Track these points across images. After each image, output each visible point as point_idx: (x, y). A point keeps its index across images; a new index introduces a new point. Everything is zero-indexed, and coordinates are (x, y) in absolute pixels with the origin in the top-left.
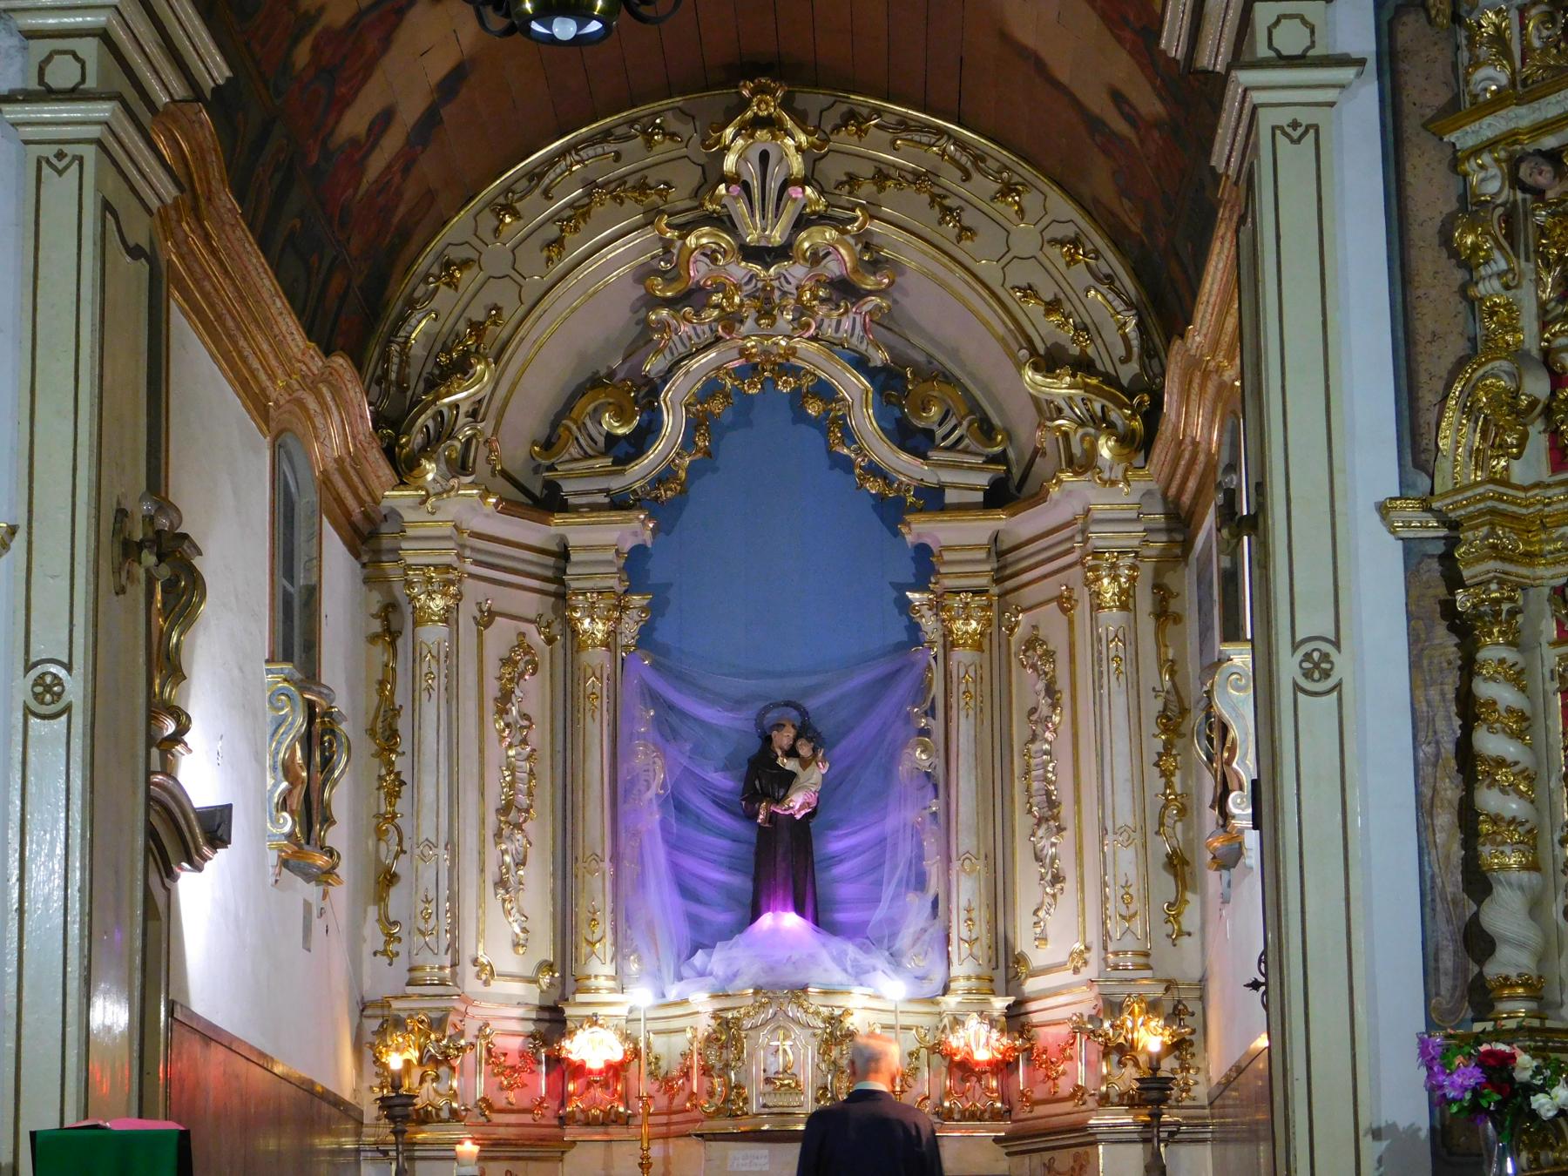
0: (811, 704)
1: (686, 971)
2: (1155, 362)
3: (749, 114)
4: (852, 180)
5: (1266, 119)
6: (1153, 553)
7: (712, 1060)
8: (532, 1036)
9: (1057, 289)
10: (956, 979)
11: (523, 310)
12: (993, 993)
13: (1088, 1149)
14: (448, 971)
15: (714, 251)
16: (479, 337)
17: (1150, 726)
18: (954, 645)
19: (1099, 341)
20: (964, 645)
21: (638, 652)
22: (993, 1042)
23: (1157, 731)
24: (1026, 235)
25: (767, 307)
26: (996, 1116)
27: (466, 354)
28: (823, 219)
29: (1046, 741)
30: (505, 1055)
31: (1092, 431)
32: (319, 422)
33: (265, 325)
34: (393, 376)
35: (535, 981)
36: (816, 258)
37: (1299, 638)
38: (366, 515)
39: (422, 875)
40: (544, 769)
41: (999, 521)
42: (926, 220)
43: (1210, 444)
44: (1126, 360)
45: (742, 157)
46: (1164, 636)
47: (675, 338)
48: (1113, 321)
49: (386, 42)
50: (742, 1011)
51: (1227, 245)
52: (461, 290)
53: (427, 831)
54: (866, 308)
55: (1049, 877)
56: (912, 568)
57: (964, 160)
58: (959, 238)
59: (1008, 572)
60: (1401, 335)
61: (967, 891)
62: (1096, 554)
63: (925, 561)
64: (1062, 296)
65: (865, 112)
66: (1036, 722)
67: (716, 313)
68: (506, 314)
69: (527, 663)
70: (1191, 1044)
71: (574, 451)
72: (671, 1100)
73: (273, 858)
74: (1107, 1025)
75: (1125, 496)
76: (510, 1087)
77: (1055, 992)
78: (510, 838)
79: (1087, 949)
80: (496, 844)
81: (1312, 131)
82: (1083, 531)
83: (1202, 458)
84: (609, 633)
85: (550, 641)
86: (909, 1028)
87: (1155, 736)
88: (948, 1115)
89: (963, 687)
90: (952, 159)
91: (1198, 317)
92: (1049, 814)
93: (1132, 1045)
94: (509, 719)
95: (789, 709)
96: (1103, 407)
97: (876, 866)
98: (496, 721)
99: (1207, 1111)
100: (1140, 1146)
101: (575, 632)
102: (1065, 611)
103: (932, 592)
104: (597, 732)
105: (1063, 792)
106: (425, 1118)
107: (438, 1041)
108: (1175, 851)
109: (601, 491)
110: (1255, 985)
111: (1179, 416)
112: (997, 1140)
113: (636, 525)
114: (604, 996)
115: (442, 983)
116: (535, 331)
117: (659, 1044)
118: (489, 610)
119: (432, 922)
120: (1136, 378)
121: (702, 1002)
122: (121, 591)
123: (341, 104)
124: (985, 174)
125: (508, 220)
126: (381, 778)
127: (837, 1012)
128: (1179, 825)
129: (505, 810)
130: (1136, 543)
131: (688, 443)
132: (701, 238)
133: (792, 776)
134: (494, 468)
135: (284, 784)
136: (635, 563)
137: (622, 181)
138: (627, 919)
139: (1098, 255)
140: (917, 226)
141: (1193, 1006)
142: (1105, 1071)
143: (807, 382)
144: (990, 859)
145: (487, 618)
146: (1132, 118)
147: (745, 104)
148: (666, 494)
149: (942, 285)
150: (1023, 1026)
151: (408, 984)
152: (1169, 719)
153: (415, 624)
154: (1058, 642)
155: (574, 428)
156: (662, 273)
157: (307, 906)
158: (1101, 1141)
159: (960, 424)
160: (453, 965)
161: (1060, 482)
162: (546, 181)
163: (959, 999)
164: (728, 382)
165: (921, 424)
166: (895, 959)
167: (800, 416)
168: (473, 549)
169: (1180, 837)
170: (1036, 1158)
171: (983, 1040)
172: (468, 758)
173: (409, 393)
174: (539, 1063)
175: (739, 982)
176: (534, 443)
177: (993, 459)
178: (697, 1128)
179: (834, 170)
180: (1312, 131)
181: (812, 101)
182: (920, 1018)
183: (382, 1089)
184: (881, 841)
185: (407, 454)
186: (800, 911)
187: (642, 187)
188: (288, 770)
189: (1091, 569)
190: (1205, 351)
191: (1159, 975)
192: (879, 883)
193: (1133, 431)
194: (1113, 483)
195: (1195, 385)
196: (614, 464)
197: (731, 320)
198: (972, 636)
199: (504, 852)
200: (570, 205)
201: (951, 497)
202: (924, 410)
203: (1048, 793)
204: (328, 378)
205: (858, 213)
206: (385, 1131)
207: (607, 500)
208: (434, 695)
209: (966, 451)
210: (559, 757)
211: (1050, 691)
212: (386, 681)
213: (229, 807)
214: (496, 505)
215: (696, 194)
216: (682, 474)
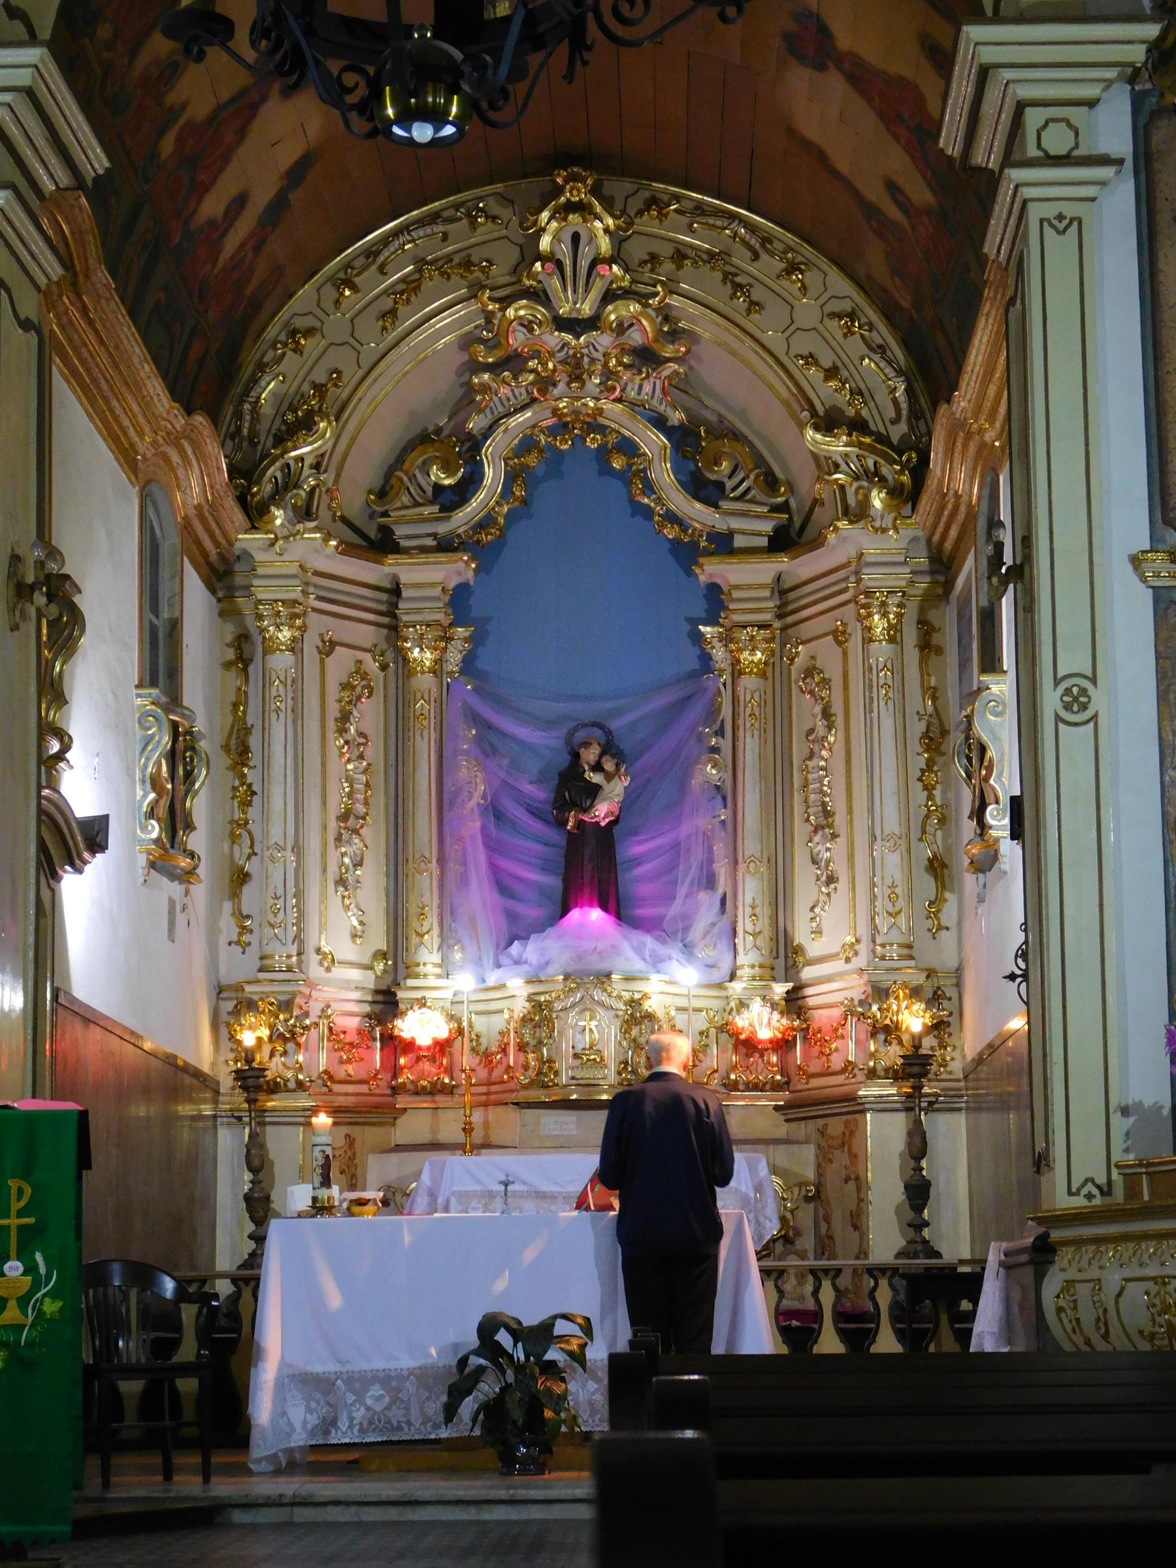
0: (614, 725)
1: (504, 959)
2: (921, 423)
3: (563, 199)
4: (654, 259)
5: (1035, 213)
6: (920, 592)
7: (527, 1038)
8: (368, 1016)
9: (835, 358)
10: (742, 966)
11: (361, 373)
12: (774, 979)
13: (857, 1116)
14: (294, 959)
15: (531, 322)
16: (322, 398)
17: (914, 745)
18: (741, 673)
19: (872, 404)
20: (751, 673)
21: (461, 679)
22: (774, 1023)
23: (921, 750)
24: (807, 309)
25: (577, 372)
26: (776, 1087)
27: (310, 414)
28: (627, 294)
29: (822, 758)
30: (344, 1033)
31: (865, 484)
32: (181, 473)
33: (136, 387)
34: (245, 432)
35: (370, 968)
36: (621, 329)
37: (1060, 674)
38: (221, 556)
39: (271, 873)
40: (379, 781)
41: (782, 563)
42: (718, 294)
43: (971, 497)
44: (896, 421)
45: (556, 238)
46: (927, 665)
47: (495, 399)
48: (883, 384)
49: (242, 134)
50: (554, 995)
51: (991, 321)
52: (305, 354)
53: (276, 835)
54: (665, 373)
55: (824, 878)
57: (753, 242)
58: (749, 312)
59: (790, 608)
60: (1152, 405)
61: (751, 890)
62: (868, 594)
63: (715, 600)
64: (839, 364)
65: (665, 198)
66: (813, 741)
67: (531, 377)
68: (345, 377)
69: (364, 687)
70: (949, 1024)
71: (406, 499)
72: (491, 1071)
73: (142, 860)
74: (875, 1008)
75: (894, 542)
76: (349, 1061)
77: (828, 979)
78: (349, 842)
79: (858, 941)
80: (337, 847)
81: (1075, 224)
82: (857, 573)
83: (963, 509)
84: (436, 662)
85: (384, 667)
86: (700, 1010)
87: (918, 754)
88: (733, 1086)
89: (748, 711)
90: (743, 241)
91: (963, 385)
92: (825, 822)
93: (897, 1026)
94: (348, 737)
95: (595, 729)
96: (875, 463)
97: (671, 867)
98: (336, 739)
99: (962, 1084)
100: (903, 1114)
101: (406, 660)
102: (840, 643)
103: (722, 626)
104: (426, 748)
105: (838, 804)
106: (274, 1088)
107: (286, 1021)
108: (935, 856)
109: (428, 535)
110: (1012, 977)
111: (943, 471)
112: (776, 1108)
113: (461, 565)
114: (432, 981)
115: (290, 970)
116: (371, 392)
117: (480, 1024)
118: (330, 641)
119: (281, 915)
120: (904, 438)
121: (518, 987)
122: (15, 628)
123: (204, 189)
124: (772, 254)
125: (347, 293)
126: (235, 789)
127: (637, 996)
128: (939, 833)
129: (344, 817)
130: (903, 583)
131: (507, 492)
132: (518, 310)
133: (597, 788)
134: (334, 514)
135: (152, 796)
136: (459, 600)
137: (449, 258)
138: (452, 914)
139: (871, 327)
140: (710, 299)
141: (950, 992)
142: (872, 1048)
143: (612, 439)
144: (772, 862)
145: (328, 647)
146: (905, 205)
147: (559, 191)
149: (734, 353)
150: (800, 1008)
151: (260, 970)
152: (931, 739)
153: (266, 652)
154: (833, 671)
155: (405, 479)
156: (483, 341)
157: (172, 902)
158: (869, 1110)
160: (299, 954)
161: (836, 529)
162: (381, 258)
163: (744, 985)
164: (543, 439)
165: (713, 477)
166: (688, 949)
167: (605, 469)
168: (316, 586)
169: (939, 842)
170: (812, 1126)
171: (765, 1021)
172: (313, 773)
173: (260, 448)
174: (375, 1039)
175: (550, 970)
176: (370, 492)
177: (775, 509)
178: (514, 1097)
179: (637, 250)
180: (1075, 224)
181: (619, 187)
182: (710, 1001)
183: (236, 1062)
184: (676, 846)
185: (258, 502)
186: (605, 908)
187: (467, 264)
188: (155, 783)
189: (866, 606)
190: (969, 414)
191: (921, 965)
192: (675, 883)
193: (902, 484)
194: (884, 530)
195: (959, 445)
196: (441, 511)
197: (545, 384)
198: (757, 665)
199: (343, 855)
200: (403, 280)
201: (739, 541)
202: (716, 464)
203: (824, 804)
204: (189, 434)
205: (659, 288)
206: (240, 1100)
207: (434, 543)
208: (282, 715)
209: (753, 501)
210: (392, 771)
211: (827, 714)
212: (239, 702)
213: (107, 816)
214: (337, 547)
215: (515, 270)
216: (501, 520)
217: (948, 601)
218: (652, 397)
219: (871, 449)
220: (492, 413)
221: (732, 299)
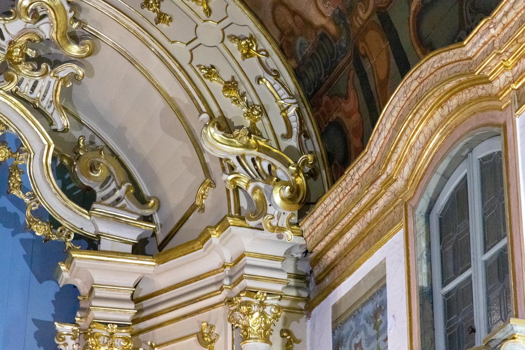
31: (261, 185)
44: (288, 136)
54: (61, 75)
56: (52, 309)
63: (70, 302)
64: (237, 79)
96: (269, 167)
103: (77, 325)
159: (120, 188)
201: (105, 244)
209: (123, 208)
217: (309, 316)
218: (43, 100)
219: (267, 151)
221: (142, 7)
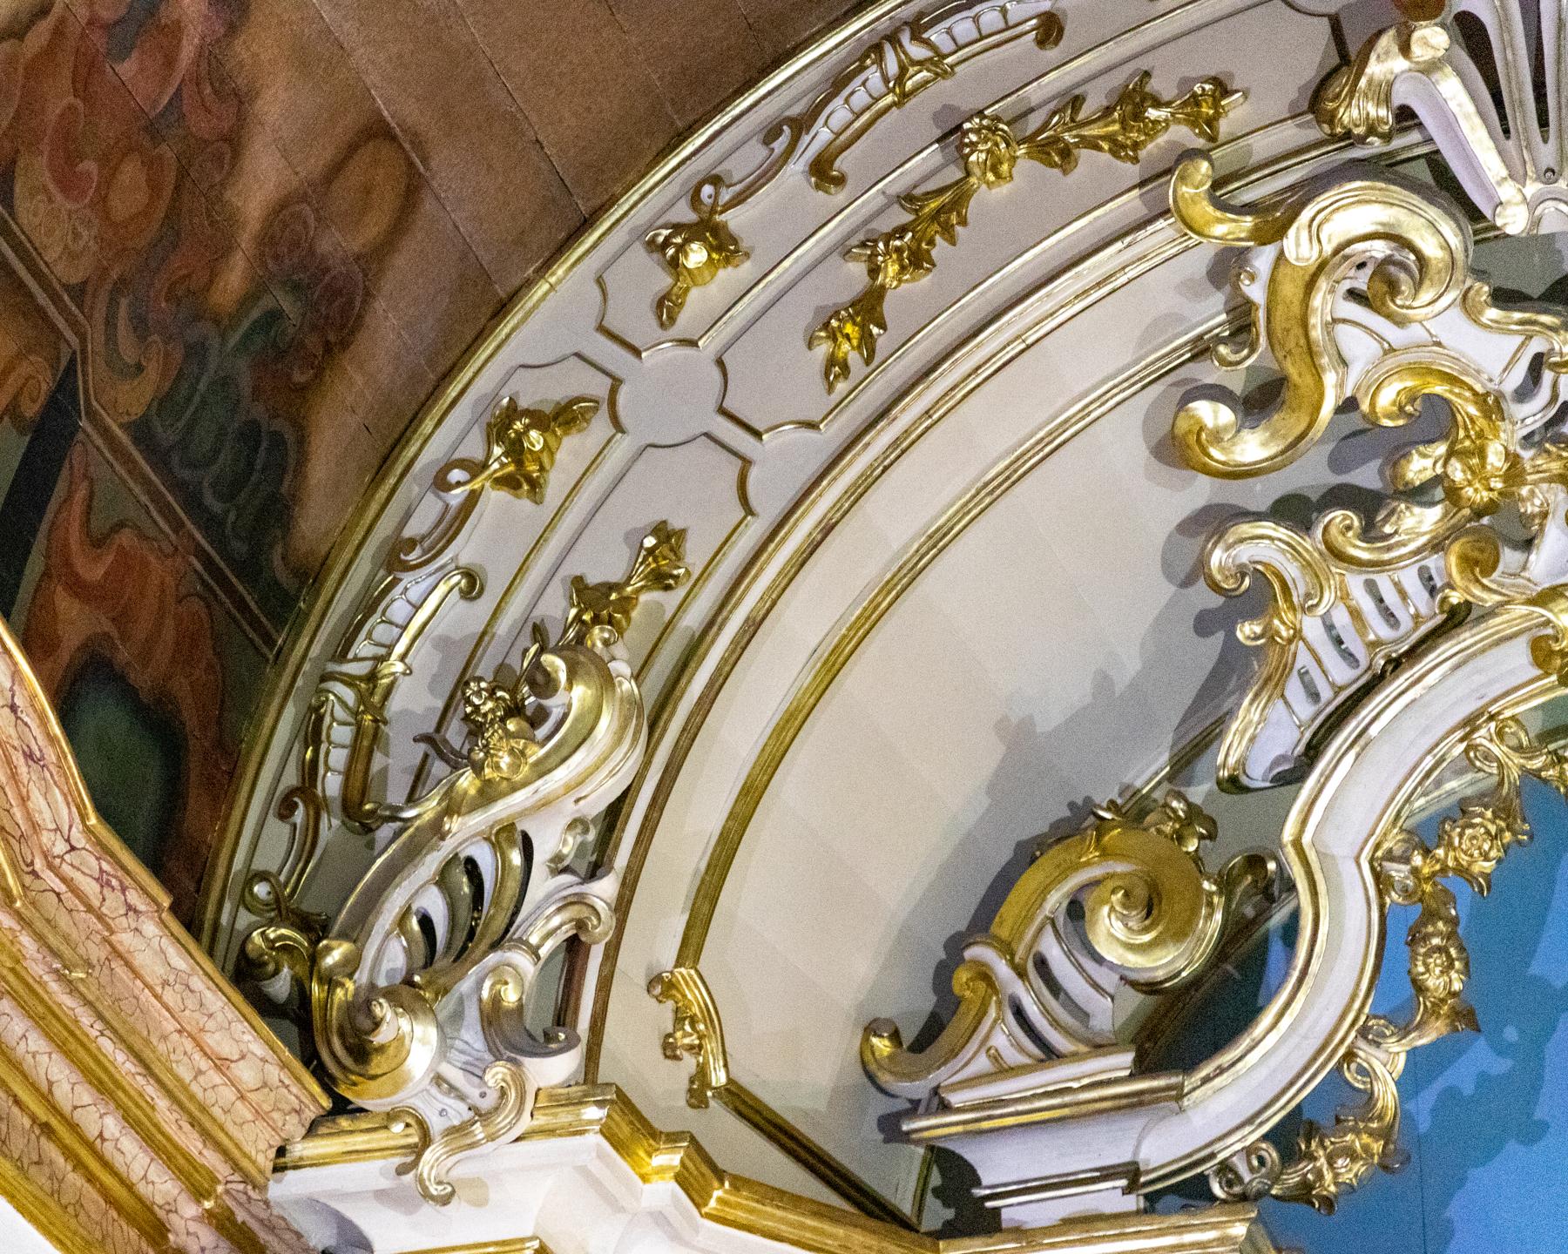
47: (1312, 628)
71: (1004, 1039)
109: (1107, 1174)
125: (697, 256)
148: (1338, 1169)
162: (821, 135)
176: (872, 1029)
220: (1314, 696)
